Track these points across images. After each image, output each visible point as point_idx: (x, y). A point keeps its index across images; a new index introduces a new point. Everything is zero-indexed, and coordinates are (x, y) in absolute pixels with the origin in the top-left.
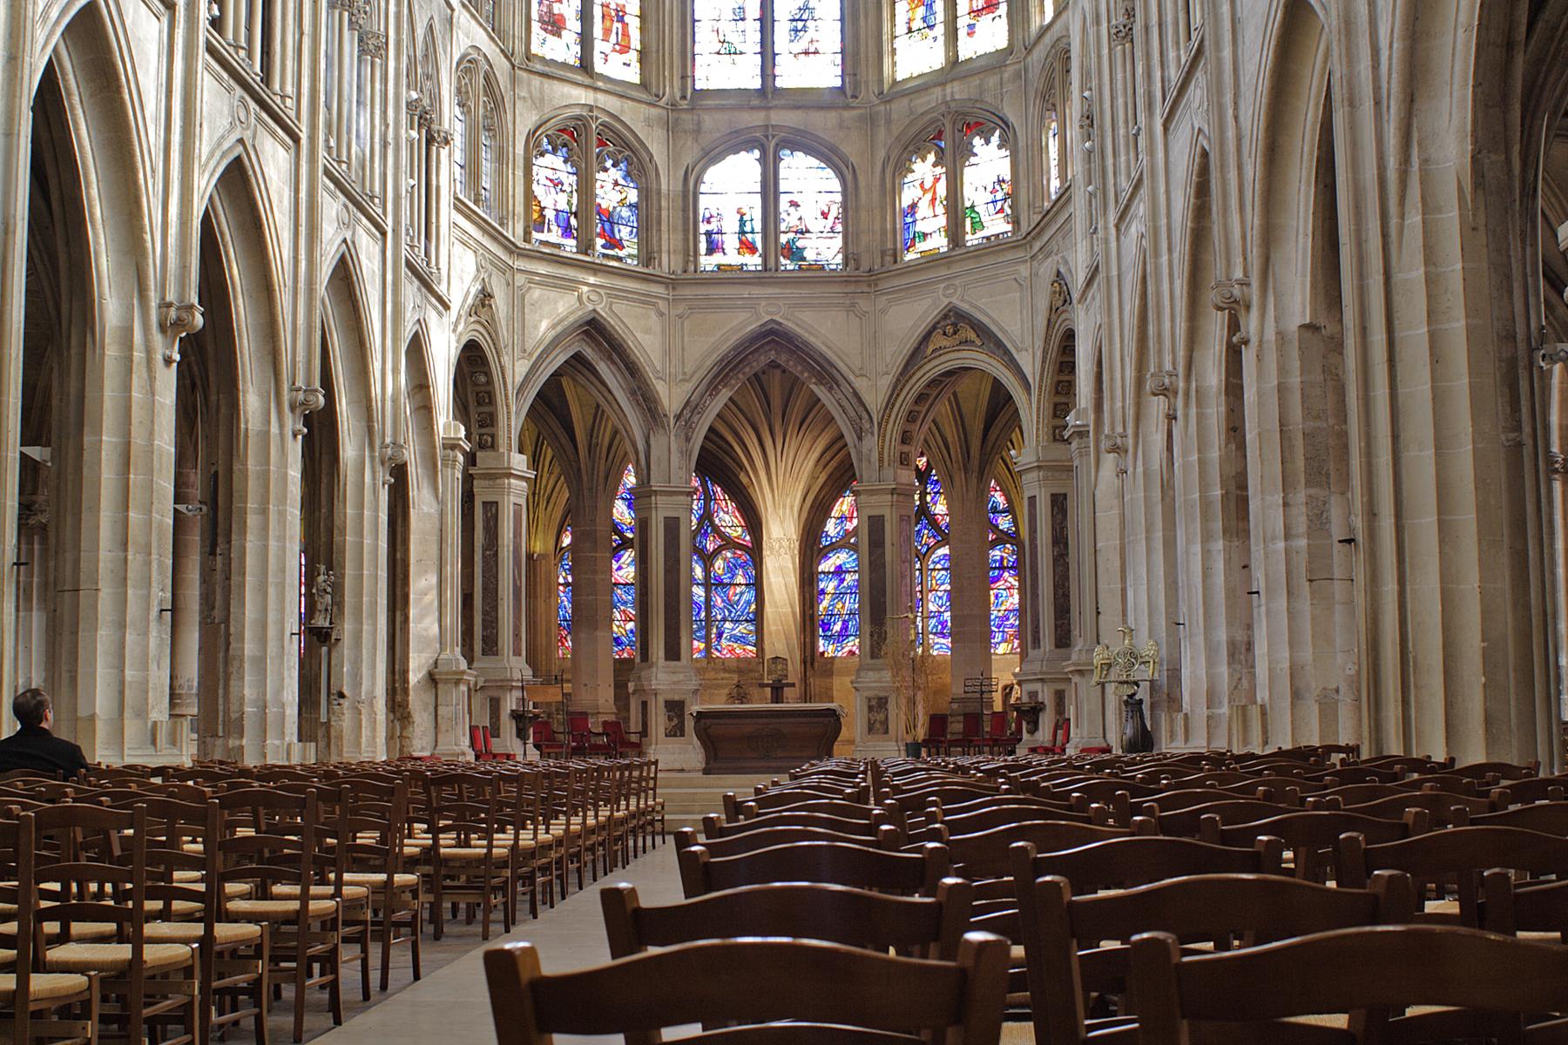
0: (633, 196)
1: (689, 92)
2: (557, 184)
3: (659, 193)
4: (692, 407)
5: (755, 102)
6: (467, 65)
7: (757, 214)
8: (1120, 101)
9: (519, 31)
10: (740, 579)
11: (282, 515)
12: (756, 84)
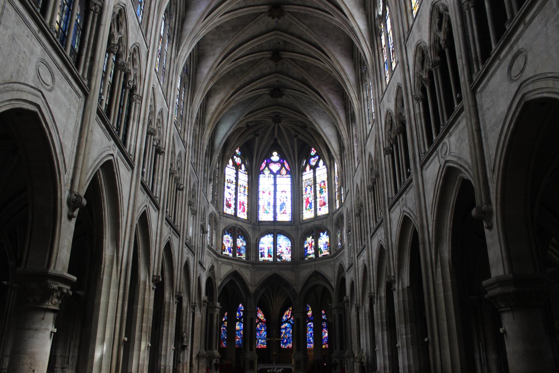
0: (245, 244)
2: (228, 241)
4: (257, 292)
6: (211, 215)
8: (357, 229)
9: (221, 208)
10: (263, 329)
11: (172, 321)
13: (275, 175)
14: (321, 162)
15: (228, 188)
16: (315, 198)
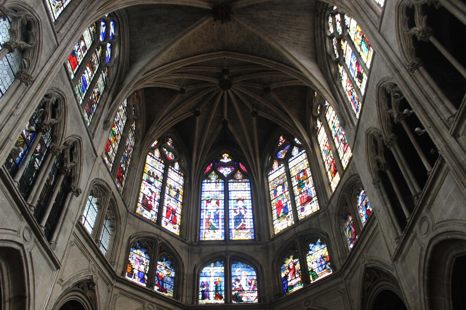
0: (173, 274)
1: (197, 241)
2: (141, 261)
3: (184, 273)
5: (223, 243)
7: (223, 284)
8: (426, 88)
12: (223, 238)
13: (226, 180)
15: (151, 183)
16: (293, 196)
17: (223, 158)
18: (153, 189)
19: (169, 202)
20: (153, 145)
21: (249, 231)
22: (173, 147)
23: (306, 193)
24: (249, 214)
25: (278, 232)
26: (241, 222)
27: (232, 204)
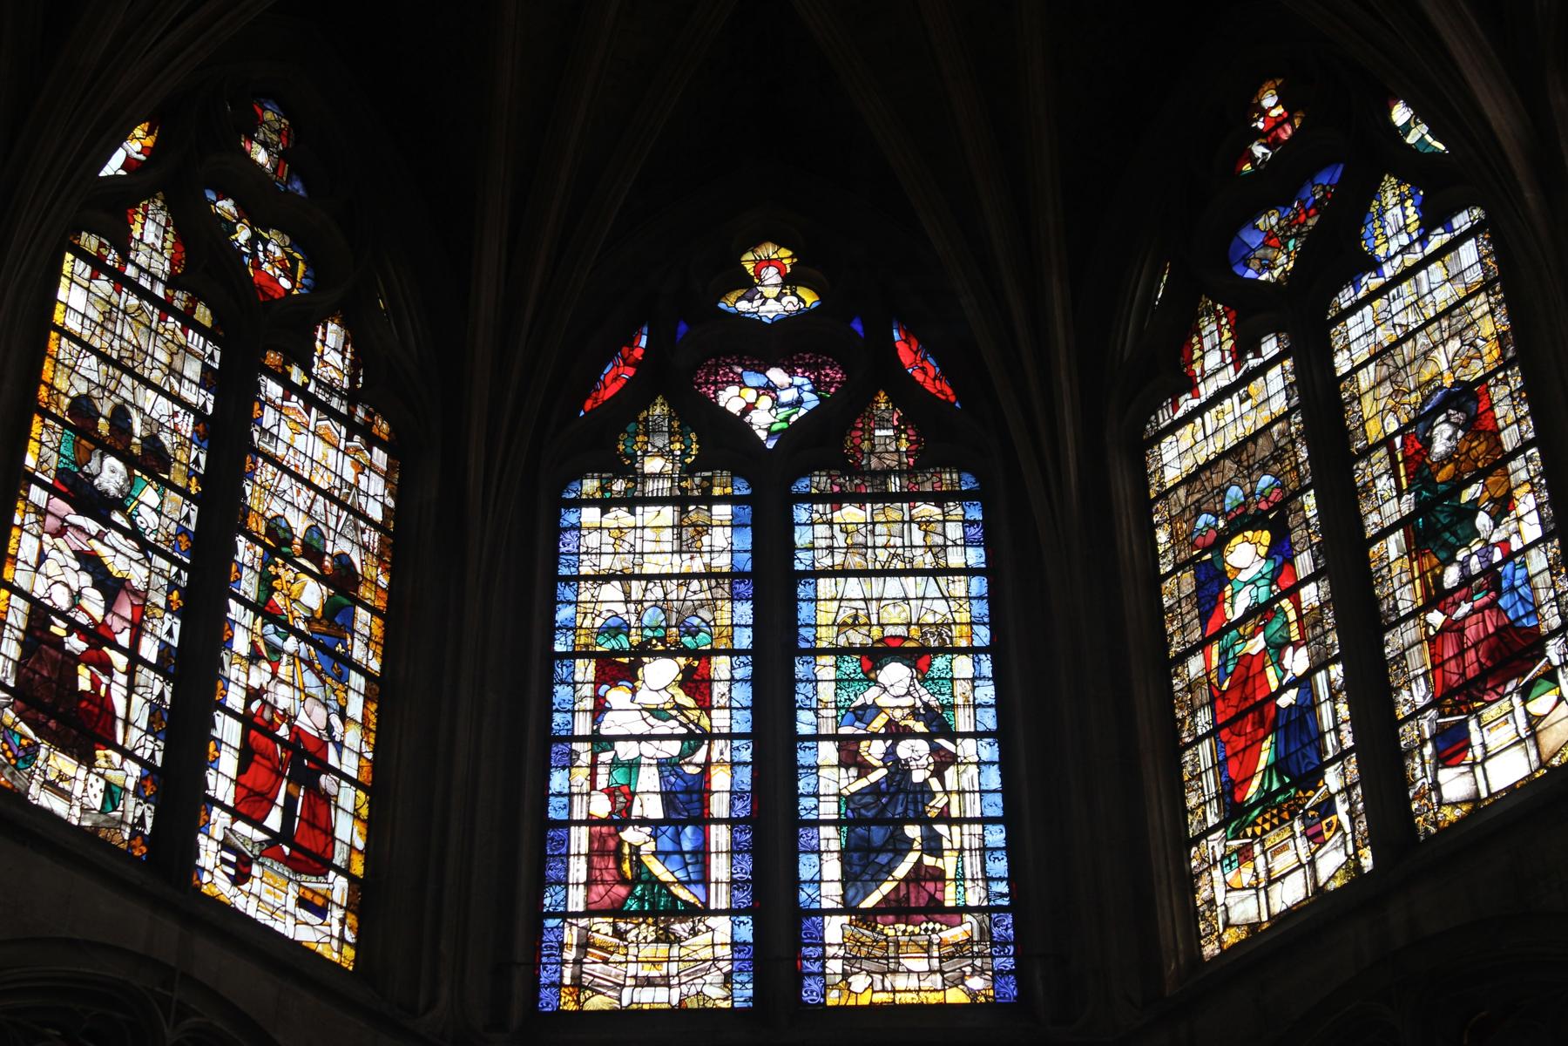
13: (772, 482)
14: (1395, 218)
15: (97, 505)
16: (1360, 619)
17: (749, 285)
18: (121, 559)
19: (259, 676)
20: (114, 166)
21: (970, 924)
22: (297, 186)
23: (1480, 599)
24: (973, 781)
25: (1230, 937)
26: (901, 847)
27: (827, 691)
